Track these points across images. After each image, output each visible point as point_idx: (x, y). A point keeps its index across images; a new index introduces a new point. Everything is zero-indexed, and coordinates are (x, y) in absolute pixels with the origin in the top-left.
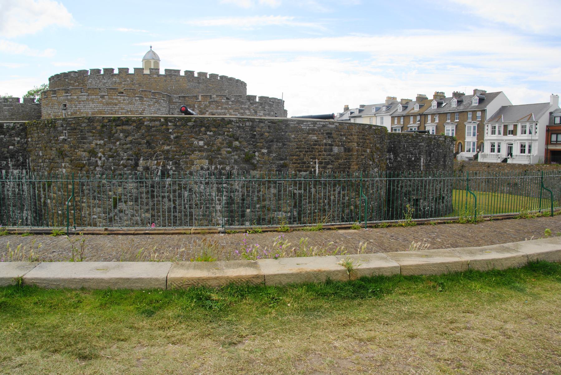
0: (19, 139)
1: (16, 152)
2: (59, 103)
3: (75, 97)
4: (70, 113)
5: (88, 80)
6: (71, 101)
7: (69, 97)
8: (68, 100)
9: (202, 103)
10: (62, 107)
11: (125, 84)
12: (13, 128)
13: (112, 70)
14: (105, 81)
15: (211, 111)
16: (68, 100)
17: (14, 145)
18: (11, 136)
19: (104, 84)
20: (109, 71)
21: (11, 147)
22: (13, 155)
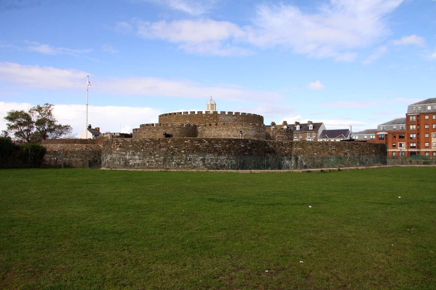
0: (289, 148)
1: (287, 153)
2: (238, 130)
3: (247, 128)
7: (243, 128)
8: (243, 129)
9: (274, 132)
10: (239, 132)
11: (239, 120)
12: (287, 144)
13: (225, 112)
14: (230, 118)
15: (278, 135)
16: (243, 129)
17: (287, 150)
18: (286, 147)
19: (229, 119)
20: (230, 113)
21: (286, 151)
22: (286, 155)
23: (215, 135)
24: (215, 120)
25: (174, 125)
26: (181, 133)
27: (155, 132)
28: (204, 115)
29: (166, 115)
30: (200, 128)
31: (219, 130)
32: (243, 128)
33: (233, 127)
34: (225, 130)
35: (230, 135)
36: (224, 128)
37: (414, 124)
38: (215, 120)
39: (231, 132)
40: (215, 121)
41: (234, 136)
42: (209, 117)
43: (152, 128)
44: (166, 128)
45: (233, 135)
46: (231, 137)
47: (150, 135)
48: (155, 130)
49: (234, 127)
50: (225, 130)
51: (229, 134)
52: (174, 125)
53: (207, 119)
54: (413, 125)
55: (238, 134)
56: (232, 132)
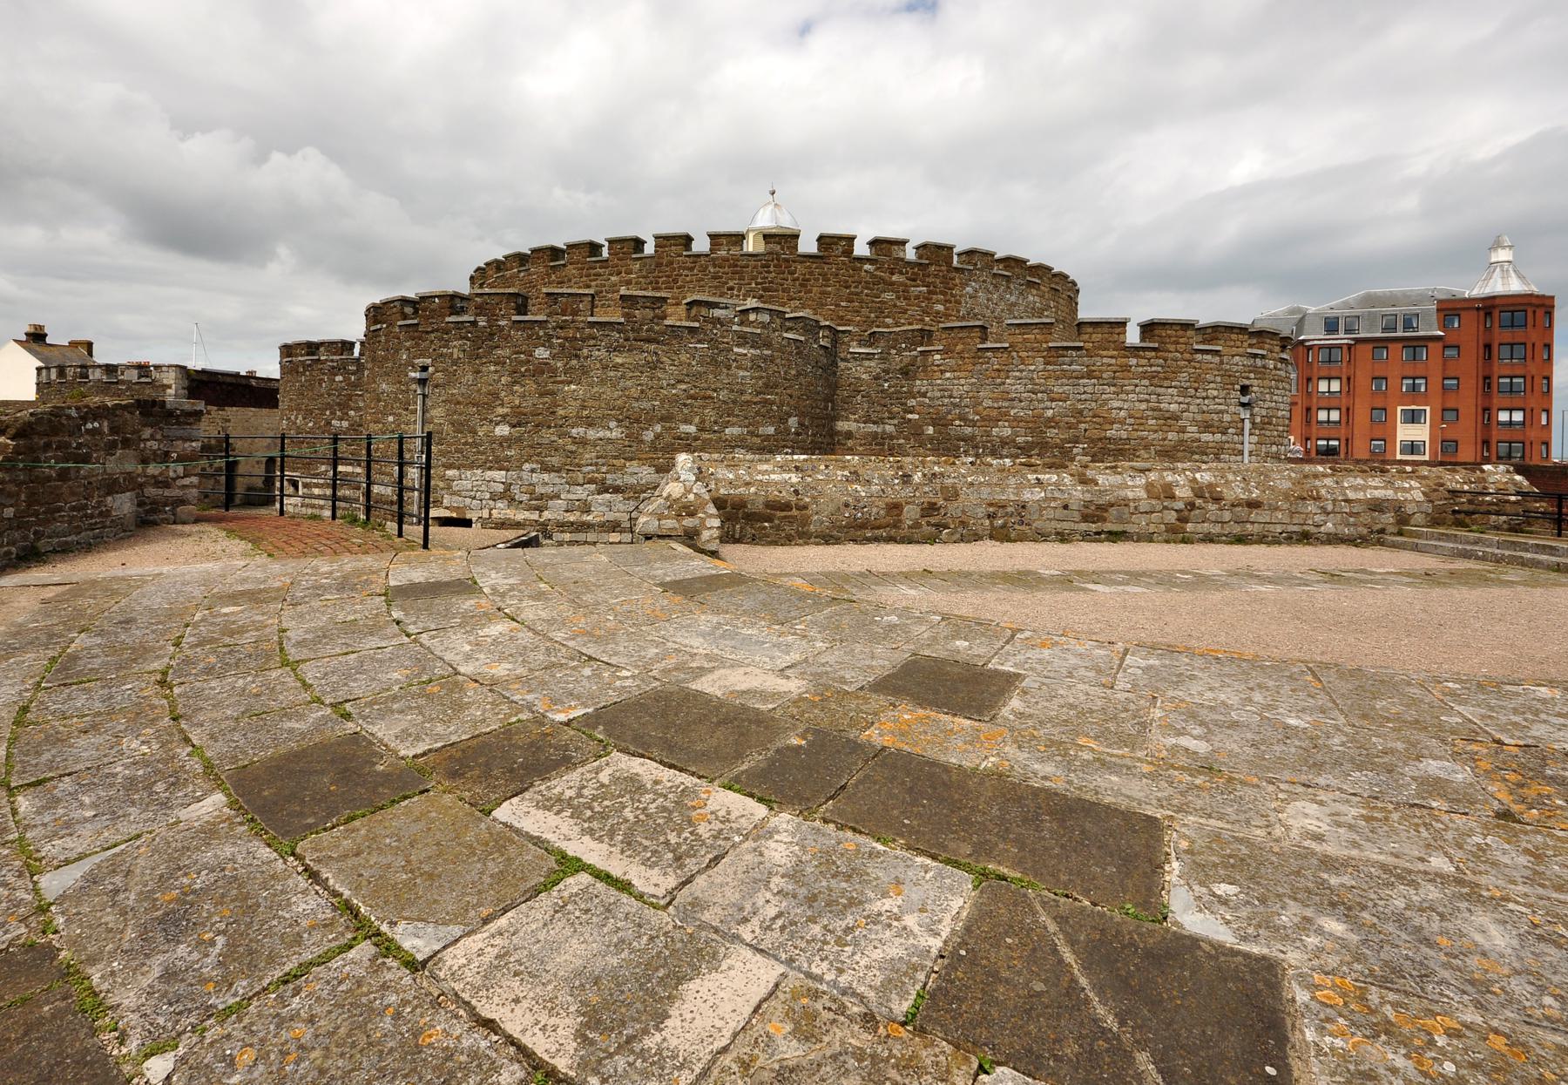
4: (1258, 420)
5: (964, 285)
6: (1261, 373)
14: (1013, 299)
23: (1050, 413)
24: (938, 302)
25: (717, 313)
26: (769, 387)
27: (541, 369)
28: (867, 267)
29: (521, 259)
30: (869, 357)
31: (1089, 375)
32: (1259, 362)
33: (1199, 357)
34: (1144, 376)
35: (1176, 417)
36: (1133, 361)
37: (1333, 374)
38: (940, 307)
39: (1183, 391)
40: (938, 312)
41: (1207, 427)
42: (902, 284)
43: (517, 335)
44: (649, 341)
45: (1199, 417)
46: (1183, 430)
47: (495, 395)
48: (542, 353)
49: (1209, 357)
50: (1144, 376)
51: (1173, 407)
52: (717, 313)
53: (888, 296)
54: (1329, 379)
55: (1232, 409)
56: (1192, 391)
